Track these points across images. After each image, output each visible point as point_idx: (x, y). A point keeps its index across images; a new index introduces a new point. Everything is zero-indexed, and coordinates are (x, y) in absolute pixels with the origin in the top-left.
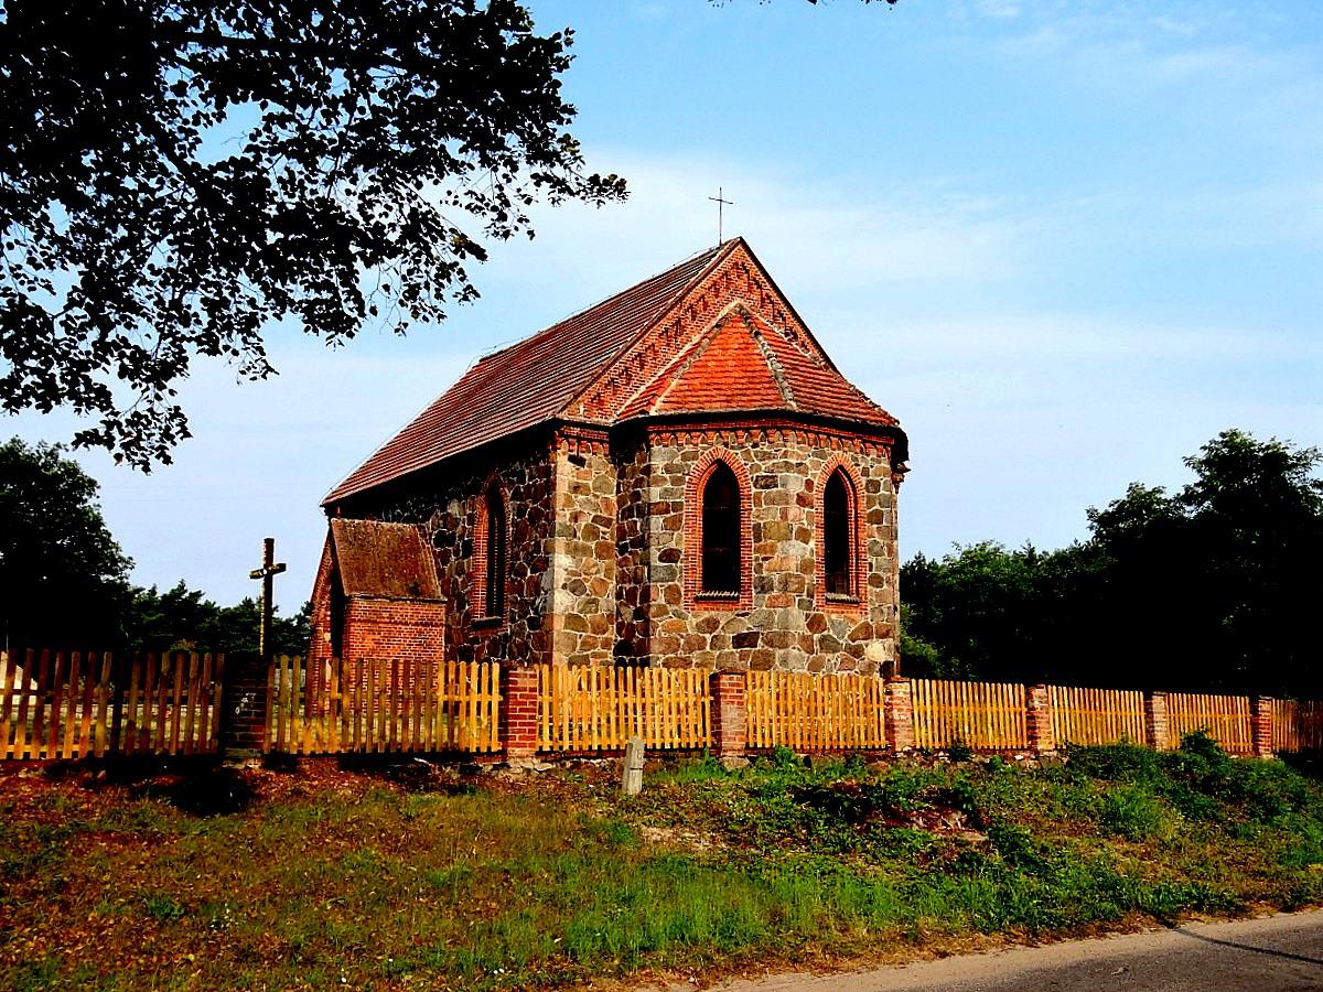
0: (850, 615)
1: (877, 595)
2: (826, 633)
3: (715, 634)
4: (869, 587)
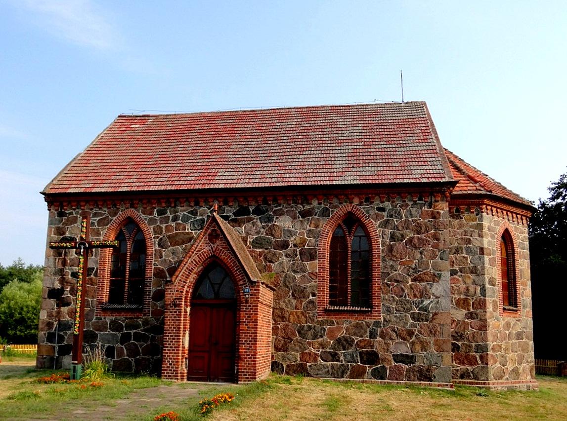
3: (510, 331)
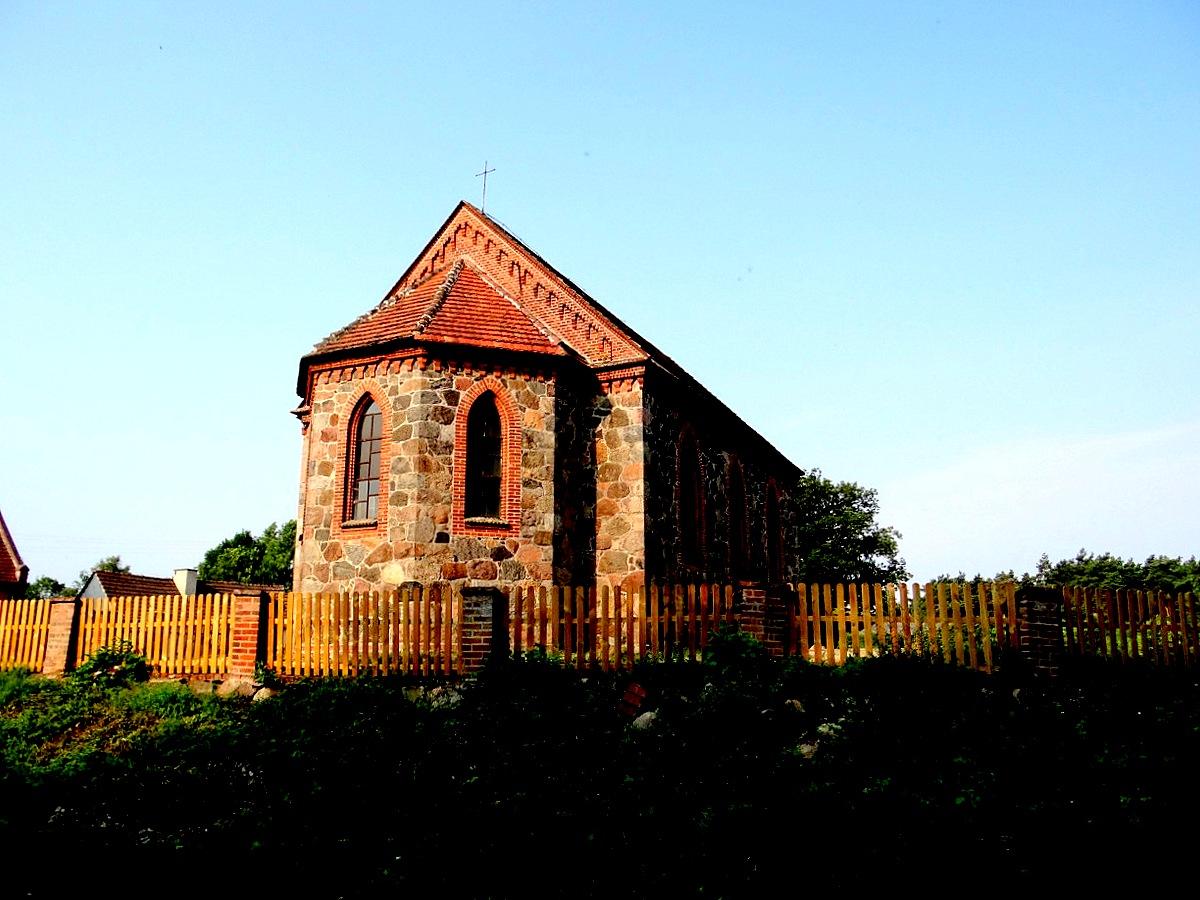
0: (367, 539)
1: (400, 514)
2: (340, 560)
4: (389, 507)
